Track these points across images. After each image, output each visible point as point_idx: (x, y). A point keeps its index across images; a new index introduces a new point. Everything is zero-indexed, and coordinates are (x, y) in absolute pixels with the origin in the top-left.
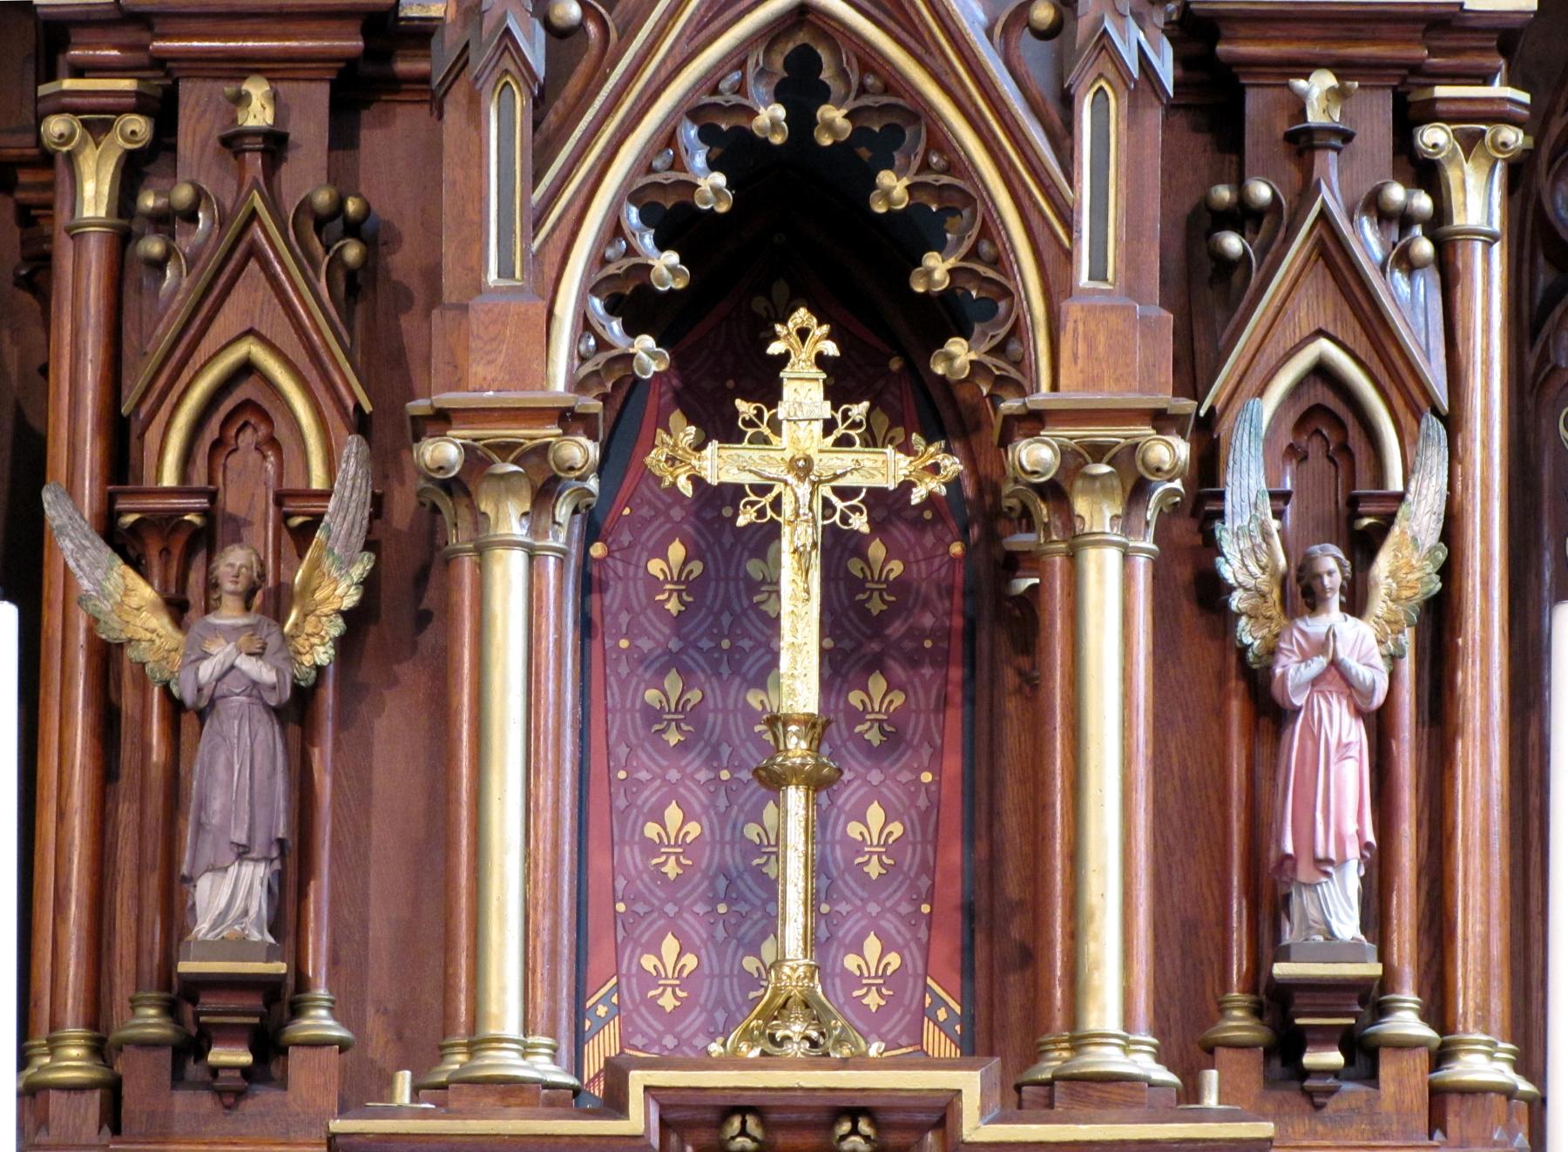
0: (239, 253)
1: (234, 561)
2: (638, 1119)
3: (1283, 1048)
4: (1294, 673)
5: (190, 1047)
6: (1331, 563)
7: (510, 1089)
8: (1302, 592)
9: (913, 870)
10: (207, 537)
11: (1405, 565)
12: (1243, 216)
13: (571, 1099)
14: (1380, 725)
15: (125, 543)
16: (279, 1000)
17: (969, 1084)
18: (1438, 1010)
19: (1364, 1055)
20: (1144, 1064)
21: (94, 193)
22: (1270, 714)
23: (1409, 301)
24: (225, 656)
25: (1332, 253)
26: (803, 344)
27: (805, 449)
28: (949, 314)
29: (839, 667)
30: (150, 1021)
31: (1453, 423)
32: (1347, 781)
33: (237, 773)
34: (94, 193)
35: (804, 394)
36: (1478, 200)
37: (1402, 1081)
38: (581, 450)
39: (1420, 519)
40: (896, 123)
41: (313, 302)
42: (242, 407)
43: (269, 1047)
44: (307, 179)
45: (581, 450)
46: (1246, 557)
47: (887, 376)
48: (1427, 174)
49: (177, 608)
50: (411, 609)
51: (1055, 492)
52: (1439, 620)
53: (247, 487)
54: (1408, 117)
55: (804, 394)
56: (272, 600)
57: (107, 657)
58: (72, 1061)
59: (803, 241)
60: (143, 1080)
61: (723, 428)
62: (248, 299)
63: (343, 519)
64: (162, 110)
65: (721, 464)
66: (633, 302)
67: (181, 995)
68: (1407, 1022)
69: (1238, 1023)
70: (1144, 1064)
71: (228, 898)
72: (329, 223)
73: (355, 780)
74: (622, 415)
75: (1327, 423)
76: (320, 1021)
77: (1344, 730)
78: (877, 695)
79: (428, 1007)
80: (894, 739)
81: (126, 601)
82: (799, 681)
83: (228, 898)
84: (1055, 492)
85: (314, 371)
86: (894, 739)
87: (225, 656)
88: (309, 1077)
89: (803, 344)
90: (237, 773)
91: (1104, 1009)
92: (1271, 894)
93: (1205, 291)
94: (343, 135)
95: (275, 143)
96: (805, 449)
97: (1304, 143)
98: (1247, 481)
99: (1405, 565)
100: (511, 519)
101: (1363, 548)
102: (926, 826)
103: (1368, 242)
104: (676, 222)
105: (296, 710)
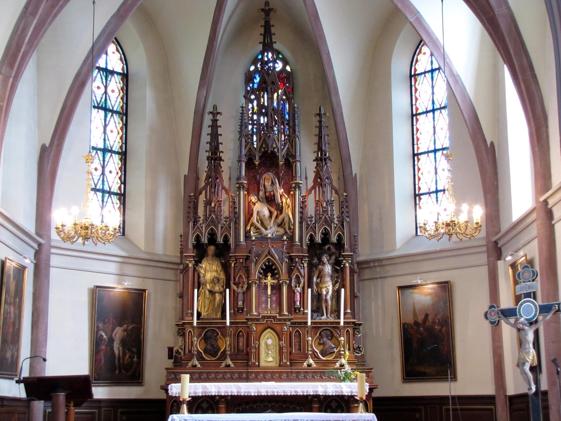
0: (240, 268)
1: (240, 285)
2: (260, 317)
3: (295, 311)
4: (296, 291)
5: (238, 311)
6: (297, 285)
7: (254, 315)
8: (296, 287)
9: (276, 301)
10: (239, 283)
11: (301, 285)
12: (293, 266)
13: (257, 316)
14: (300, 294)
15: (235, 284)
16: (243, 308)
17: (277, 315)
18: (303, 308)
19: (300, 311)
20: (287, 313)
21: (233, 265)
22: (294, 293)
23: (302, 271)
24: (240, 290)
25: (298, 268)
26: (269, 275)
27: (269, 281)
28: (277, 274)
29: (272, 290)
30: (236, 309)
31: (304, 277)
32: (298, 296)
33: (241, 297)
34: (233, 265)
35: (269, 278)
36: (305, 265)
37: (301, 312)
38: (258, 282)
39: (302, 283)
40: (273, 264)
41: (244, 271)
42: (241, 276)
43: (243, 311)
44: (244, 265)
45: (258, 282)
46: (293, 284)
47: (273, 276)
48: (303, 264)
49: (237, 287)
50: (249, 287)
51: (282, 284)
52: (303, 288)
53: (241, 281)
54: (302, 260)
55: (269, 278)
56: (242, 287)
57: (234, 290)
58: (232, 311)
59: (270, 269)
60: (236, 312)
61: (265, 279)
62: (241, 271)
63: (246, 283)
64: (236, 260)
65: (265, 281)
66: (260, 273)
67: (238, 308)
68: (302, 309)
69: (293, 309)
70: (287, 313)
71: (240, 303)
72: (245, 267)
73: (247, 297)
74: (260, 279)
75: (298, 277)
76: (245, 309)
77: (298, 294)
78: (274, 291)
79: (250, 310)
80: (275, 294)
81: (234, 287)
82: (269, 293)
83: (240, 303)
84: (282, 284)
85: (244, 275)
86: (275, 294)
87: (240, 290)
88: (245, 312)
89: (269, 275)
90: (241, 297)
91: (285, 311)
92: (295, 303)
93: (290, 271)
94: (246, 261)
95: (242, 263)
96: (269, 281)
97: (296, 262)
98: (293, 281)
99: (301, 285)
100: (254, 285)
101: (299, 284)
102: (277, 298)
103: (300, 267)
104: (262, 269)
105: (244, 293)
